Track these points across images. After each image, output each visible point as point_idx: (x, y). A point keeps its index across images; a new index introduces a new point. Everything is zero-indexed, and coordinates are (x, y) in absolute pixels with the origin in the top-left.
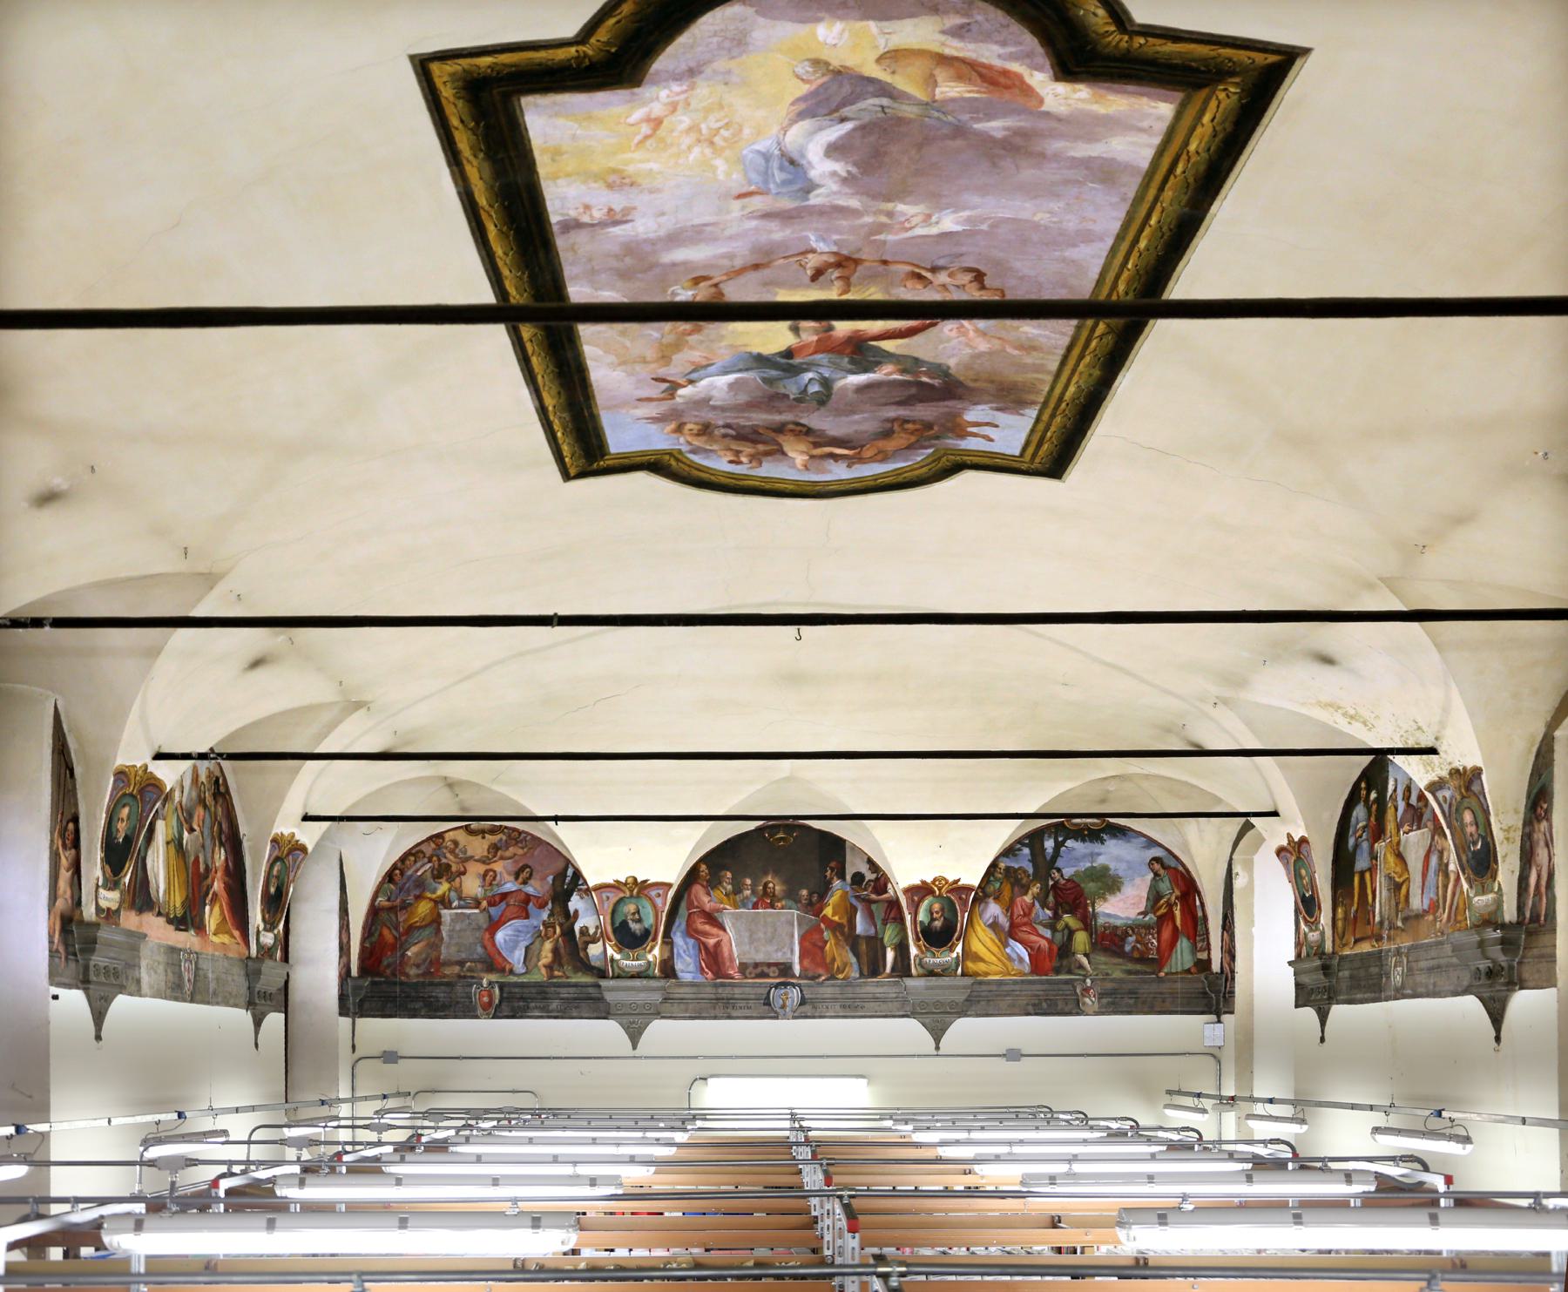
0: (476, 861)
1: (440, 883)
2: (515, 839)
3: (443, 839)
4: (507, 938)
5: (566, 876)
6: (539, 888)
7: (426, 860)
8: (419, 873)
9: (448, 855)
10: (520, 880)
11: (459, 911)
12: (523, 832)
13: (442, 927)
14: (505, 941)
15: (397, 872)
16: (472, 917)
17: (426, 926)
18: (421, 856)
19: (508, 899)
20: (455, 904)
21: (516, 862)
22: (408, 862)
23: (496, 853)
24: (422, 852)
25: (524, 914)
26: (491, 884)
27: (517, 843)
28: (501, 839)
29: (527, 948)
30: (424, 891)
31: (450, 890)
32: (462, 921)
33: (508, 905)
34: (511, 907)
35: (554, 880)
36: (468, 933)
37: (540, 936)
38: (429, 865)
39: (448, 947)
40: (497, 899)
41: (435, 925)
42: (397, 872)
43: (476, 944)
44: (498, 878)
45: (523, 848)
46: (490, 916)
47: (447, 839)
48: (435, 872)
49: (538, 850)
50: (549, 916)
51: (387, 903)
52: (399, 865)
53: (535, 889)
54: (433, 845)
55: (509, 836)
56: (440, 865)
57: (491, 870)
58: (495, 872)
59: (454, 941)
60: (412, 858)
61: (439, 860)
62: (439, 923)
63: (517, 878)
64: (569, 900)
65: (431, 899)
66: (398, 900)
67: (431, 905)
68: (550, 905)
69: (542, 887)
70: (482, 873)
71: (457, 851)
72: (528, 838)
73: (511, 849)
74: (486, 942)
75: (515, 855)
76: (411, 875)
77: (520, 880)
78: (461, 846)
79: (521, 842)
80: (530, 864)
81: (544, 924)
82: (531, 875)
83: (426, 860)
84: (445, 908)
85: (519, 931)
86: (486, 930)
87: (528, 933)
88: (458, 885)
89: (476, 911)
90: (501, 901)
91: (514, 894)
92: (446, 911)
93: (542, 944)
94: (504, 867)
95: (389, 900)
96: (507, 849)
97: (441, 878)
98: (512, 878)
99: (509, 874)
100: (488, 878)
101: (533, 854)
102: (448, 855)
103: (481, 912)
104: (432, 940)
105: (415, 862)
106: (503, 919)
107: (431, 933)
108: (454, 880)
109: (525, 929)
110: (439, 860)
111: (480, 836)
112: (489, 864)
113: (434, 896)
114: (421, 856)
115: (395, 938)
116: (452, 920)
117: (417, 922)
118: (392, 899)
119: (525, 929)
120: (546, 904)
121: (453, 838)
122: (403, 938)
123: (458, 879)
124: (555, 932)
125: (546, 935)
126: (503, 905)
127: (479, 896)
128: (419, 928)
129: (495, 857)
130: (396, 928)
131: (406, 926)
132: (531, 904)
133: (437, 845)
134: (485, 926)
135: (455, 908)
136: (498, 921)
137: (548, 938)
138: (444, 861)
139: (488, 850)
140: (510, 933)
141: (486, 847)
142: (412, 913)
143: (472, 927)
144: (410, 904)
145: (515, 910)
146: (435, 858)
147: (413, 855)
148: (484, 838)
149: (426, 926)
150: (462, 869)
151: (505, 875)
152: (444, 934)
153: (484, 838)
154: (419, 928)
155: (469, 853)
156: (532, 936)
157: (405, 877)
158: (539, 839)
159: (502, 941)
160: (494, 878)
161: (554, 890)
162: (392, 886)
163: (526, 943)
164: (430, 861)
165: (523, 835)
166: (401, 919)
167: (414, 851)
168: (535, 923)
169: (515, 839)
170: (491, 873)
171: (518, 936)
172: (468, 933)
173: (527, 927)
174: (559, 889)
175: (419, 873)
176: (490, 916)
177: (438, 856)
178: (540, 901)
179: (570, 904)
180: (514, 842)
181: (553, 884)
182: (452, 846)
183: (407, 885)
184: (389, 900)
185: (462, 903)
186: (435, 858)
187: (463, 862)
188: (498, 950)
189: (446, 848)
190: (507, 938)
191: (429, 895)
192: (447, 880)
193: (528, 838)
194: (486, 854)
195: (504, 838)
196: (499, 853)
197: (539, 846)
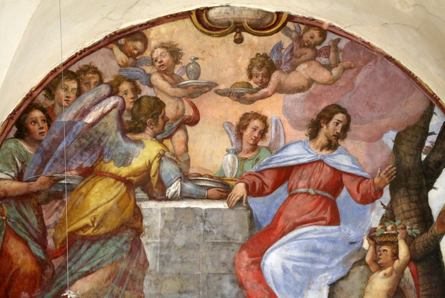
0: (217, 92)
1: (139, 142)
2: (313, 47)
3: (145, 41)
4: (289, 265)
5: (426, 133)
6: (363, 158)
7: (104, 89)
8: (89, 119)
9: (157, 79)
10: (322, 139)
11: (183, 204)
12: (332, 29)
13: (144, 239)
14: (285, 270)
15: (37, 114)
16: (213, 219)
17: (108, 236)
18: (96, 78)
19: (294, 178)
20: (173, 189)
21: (313, 98)
22: (61, 93)
23: (268, 75)
24: (96, 71)
25: (327, 215)
26: (255, 147)
27: (317, 54)
28: (279, 47)
29: (333, 286)
30: (101, 156)
31: (161, 157)
32: (189, 227)
33: (292, 194)
34: (299, 200)
35: (398, 141)
36: (203, 252)
37: (362, 262)
38: (113, 101)
39: (157, 283)
40: (269, 180)
41: (127, 235)
42: (37, 114)
43: (220, 276)
44: (271, 133)
45: (329, 67)
46: (251, 217)
47: (153, 43)
48: (127, 118)
49: (364, 72)
50: (384, 220)
51: (16, 185)
52: (41, 98)
53: (355, 160)
54: (120, 56)
55: (300, 37)
56: (138, 102)
57: (256, 115)
58: (264, 119)
59: (169, 271)
60: (73, 85)
61: (136, 90)
62: (139, 231)
63: (313, 135)
64: (430, 186)
65: (118, 178)
66: (42, 179)
67: (121, 188)
68: (386, 196)
69: (370, 155)
70: (235, 121)
71: (177, 70)
72: (343, 44)
73: (302, 68)
74: (243, 273)
75: (311, 82)
76: (71, 124)
77: (322, 139)
78: (185, 60)
79: (326, 52)
80: (344, 104)
81: (371, 237)
82: (346, 128)
83: (104, 89)
84: (152, 198)
85: (316, 251)
86: (244, 246)
87: (335, 254)
88: (180, 148)
89: (222, 205)
90: (277, 185)
91: (307, 171)
92: (152, 204)
93: (367, 280)
94: (286, 110)
95: (19, 177)
96: (294, 67)
97: (141, 131)
98: (303, 135)
99: (296, 125)
100: (247, 133)
101: (351, 83)
102: (157, 79)
103: (231, 208)
104: (123, 266)
105: (79, 93)
106: (281, 223)
107: (119, 251)
108: (170, 137)
109: (330, 247)
110: (136, 90)
111: (231, 38)
112: (252, 101)
113: (124, 171)
114: (96, 78)
115: (39, 262)
116: (167, 223)
117: (87, 226)
118: (28, 174)
119: (330, 247)
120: (379, 193)
121: (166, 39)
122: (56, 262)
123: (179, 136)
124: (395, 256)
125: (375, 260)
126: (282, 191)
127: (228, 174)
128: (93, 240)
129: (264, 85)
130: (43, 245)
131: (61, 237)
132: (344, 193)
133: (129, 54)
134: (240, 238)
135: (172, 199)
136: (272, 227)
137: (381, 268)
138: (146, 91)
139: (250, 70)
140: (296, 253)
141: (245, 63)
142: (74, 207)
143: (209, 239)
144: (71, 189)
145: (309, 203)
146: (125, 86)
147: (74, 76)
148: (239, 41)
149: (108, 236)
150: (189, 112)
151: (288, 128)
152: (150, 256)
153: (239, 41)
154: (93, 240)
155: (204, 78)
156: (346, 260)
157: (56, 129)
158: (367, 46)
159: (279, 270)
160: (263, 134)
161: (398, 164)
162: (26, 147)
163: (331, 277)
164: (114, 92)
165: (331, 37)
166: (49, 222)
167: (74, 68)
168: (353, 235)
169: (313, 47)
170: (256, 123)
171: (313, 261)
172: (203, 252)
173: (334, 241)
174: (408, 162)
175: (89, 119)
176: (251, 217)
177: (132, 81)
178: (364, 185)
179: (432, 194)
180: (309, 53)
181: (396, 149)
182: (166, 59)
183: (61, 147)
184: (19, 177)
185: (189, 186)
186: (125, 86)
187: (191, 96)
188: (268, 288)
189: (153, 62)
190: (289, 265)
191: (112, 168)
192: (154, 136)
193: (343, 44)
194: (244, 78)
195: (287, 42)
196: (275, 76)
197: (366, 62)
